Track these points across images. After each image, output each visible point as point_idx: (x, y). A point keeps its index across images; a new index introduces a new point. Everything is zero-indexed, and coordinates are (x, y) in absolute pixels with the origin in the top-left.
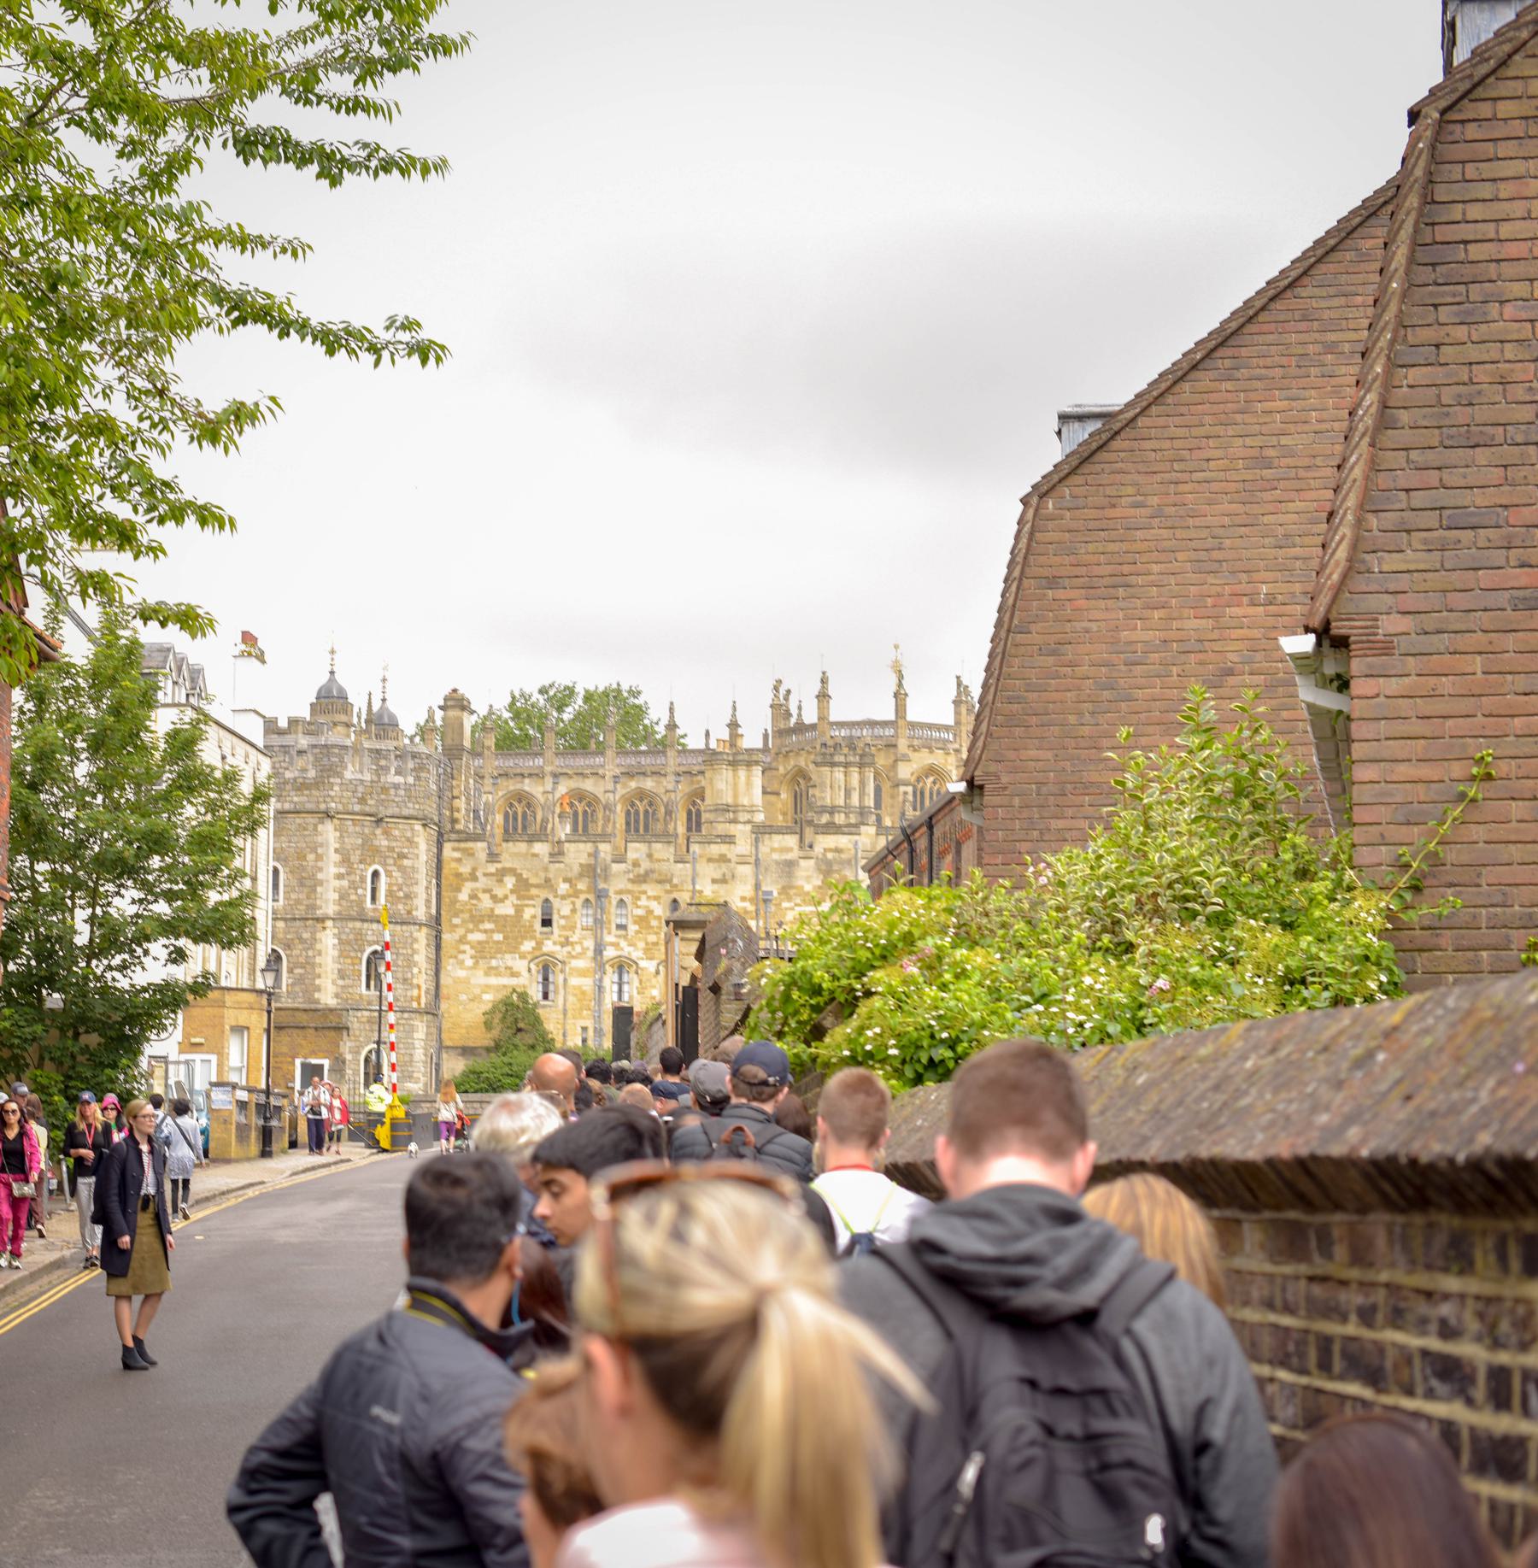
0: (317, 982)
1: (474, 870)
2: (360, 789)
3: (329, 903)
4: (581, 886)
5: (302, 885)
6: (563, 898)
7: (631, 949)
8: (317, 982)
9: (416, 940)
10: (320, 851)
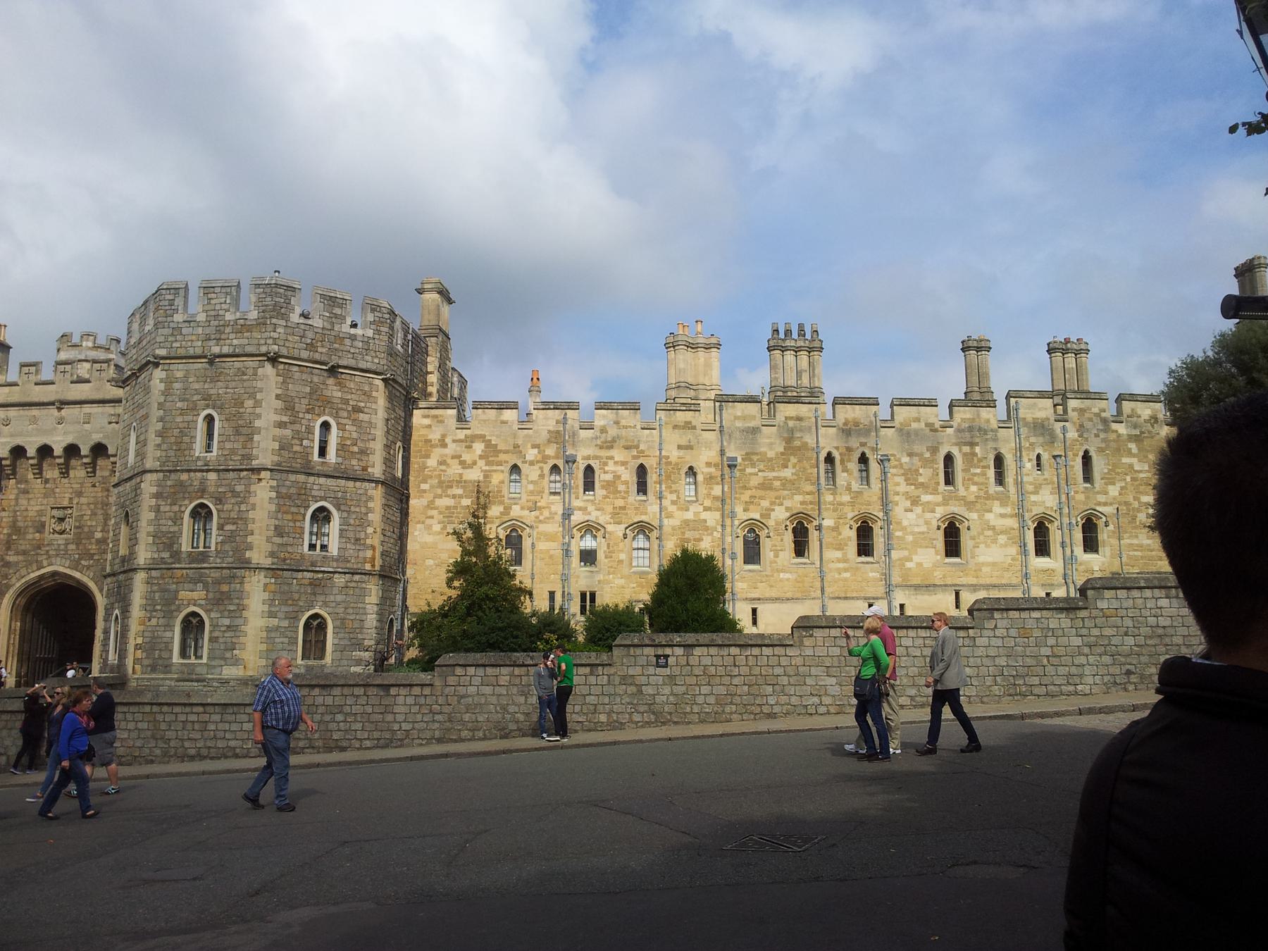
0: (249, 539)
1: (444, 436)
2: (310, 334)
3: (265, 451)
4: (551, 451)
5: (237, 432)
6: (532, 463)
7: (599, 513)
8: (249, 539)
9: (371, 498)
10: (259, 396)
